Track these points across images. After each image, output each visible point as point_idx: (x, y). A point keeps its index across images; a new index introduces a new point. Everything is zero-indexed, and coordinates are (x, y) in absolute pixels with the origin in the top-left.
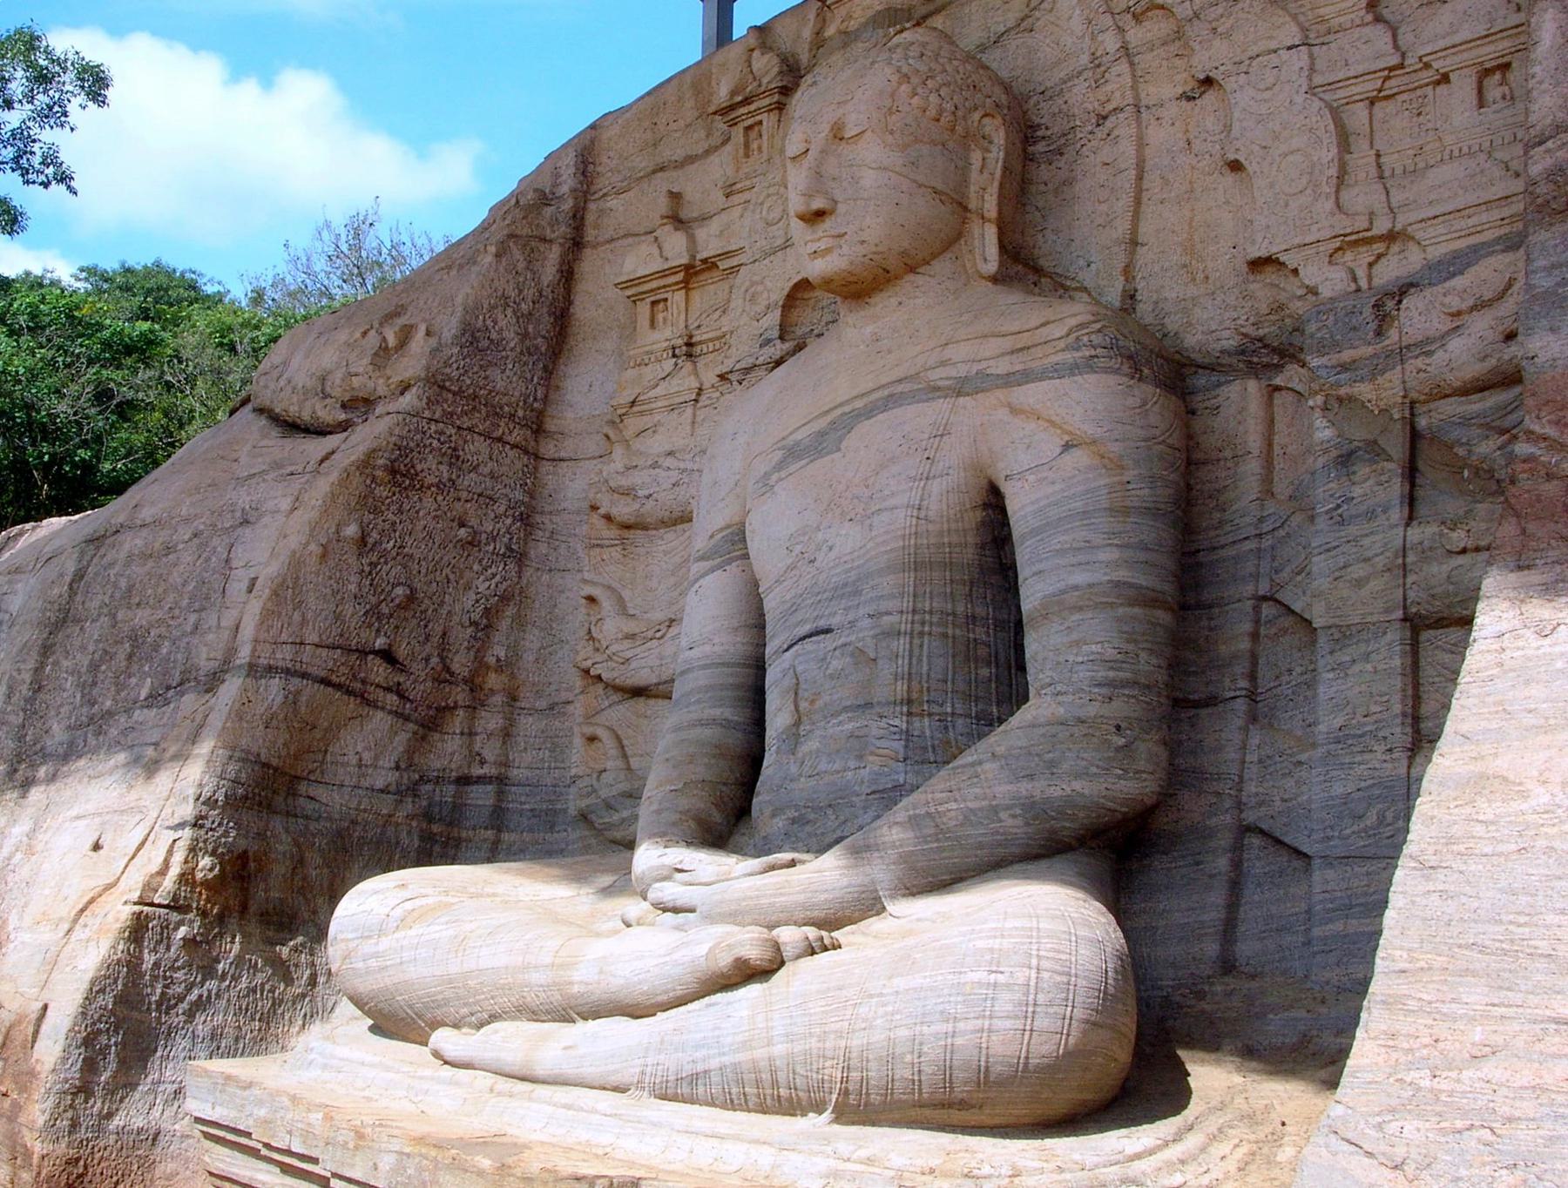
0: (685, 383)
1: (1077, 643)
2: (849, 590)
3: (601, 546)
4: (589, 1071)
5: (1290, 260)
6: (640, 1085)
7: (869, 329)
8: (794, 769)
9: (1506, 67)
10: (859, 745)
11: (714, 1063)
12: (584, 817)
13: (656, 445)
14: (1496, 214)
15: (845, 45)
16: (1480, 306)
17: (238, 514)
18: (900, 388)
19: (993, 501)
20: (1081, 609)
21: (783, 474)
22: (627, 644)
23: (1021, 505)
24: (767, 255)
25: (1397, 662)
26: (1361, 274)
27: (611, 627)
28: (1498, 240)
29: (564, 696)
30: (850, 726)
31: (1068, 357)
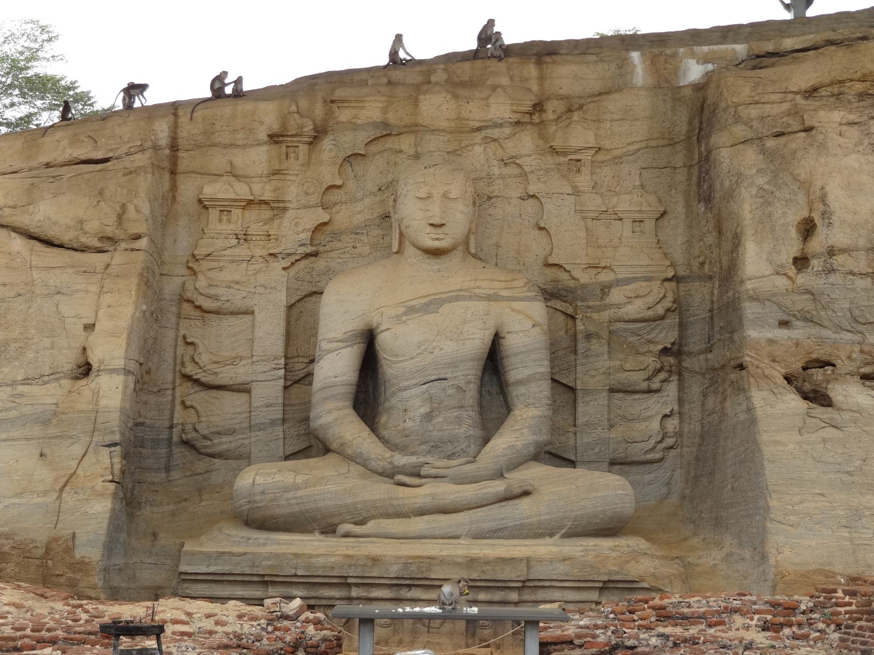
0: (243, 251)
1: (540, 391)
2: (453, 365)
3: (190, 319)
4: (437, 533)
5: (568, 268)
6: (466, 535)
7: (437, 267)
8: (431, 428)
9: (641, 221)
10: (459, 420)
11: (511, 524)
12: (186, 443)
13: (224, 276)
14: (643, 270)
15: (355, 130)
16: (636, 297)
17: (53, 288)
18: (461, 293)
19: (497, 339)
20: (541, 380)
21: (409, 317)
22: (215, 366)
23: (513, 343)
24: (305, 207)
25: (606, 402)
26: (593, 277)
27: (204, 358)
28: (642, 277)
29: (165, 386)
30: (456, 414)
31: (529, 294)
